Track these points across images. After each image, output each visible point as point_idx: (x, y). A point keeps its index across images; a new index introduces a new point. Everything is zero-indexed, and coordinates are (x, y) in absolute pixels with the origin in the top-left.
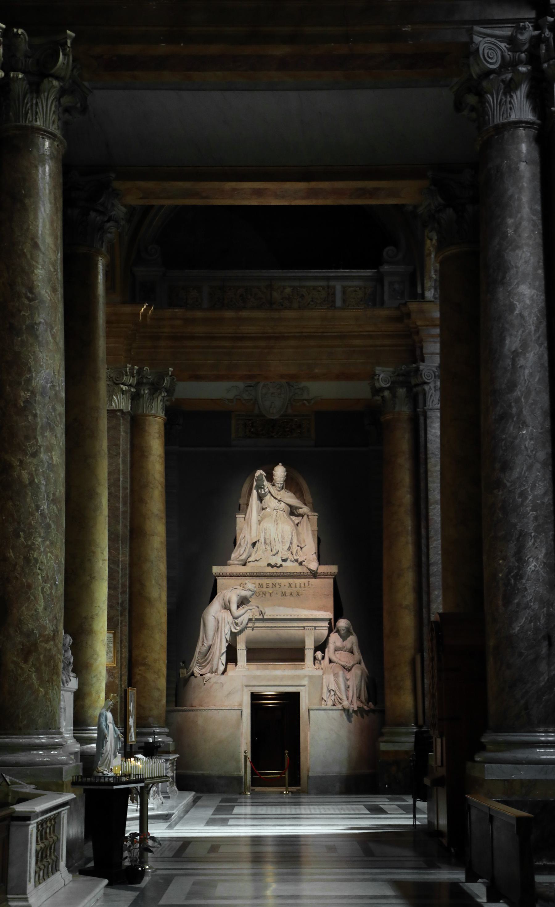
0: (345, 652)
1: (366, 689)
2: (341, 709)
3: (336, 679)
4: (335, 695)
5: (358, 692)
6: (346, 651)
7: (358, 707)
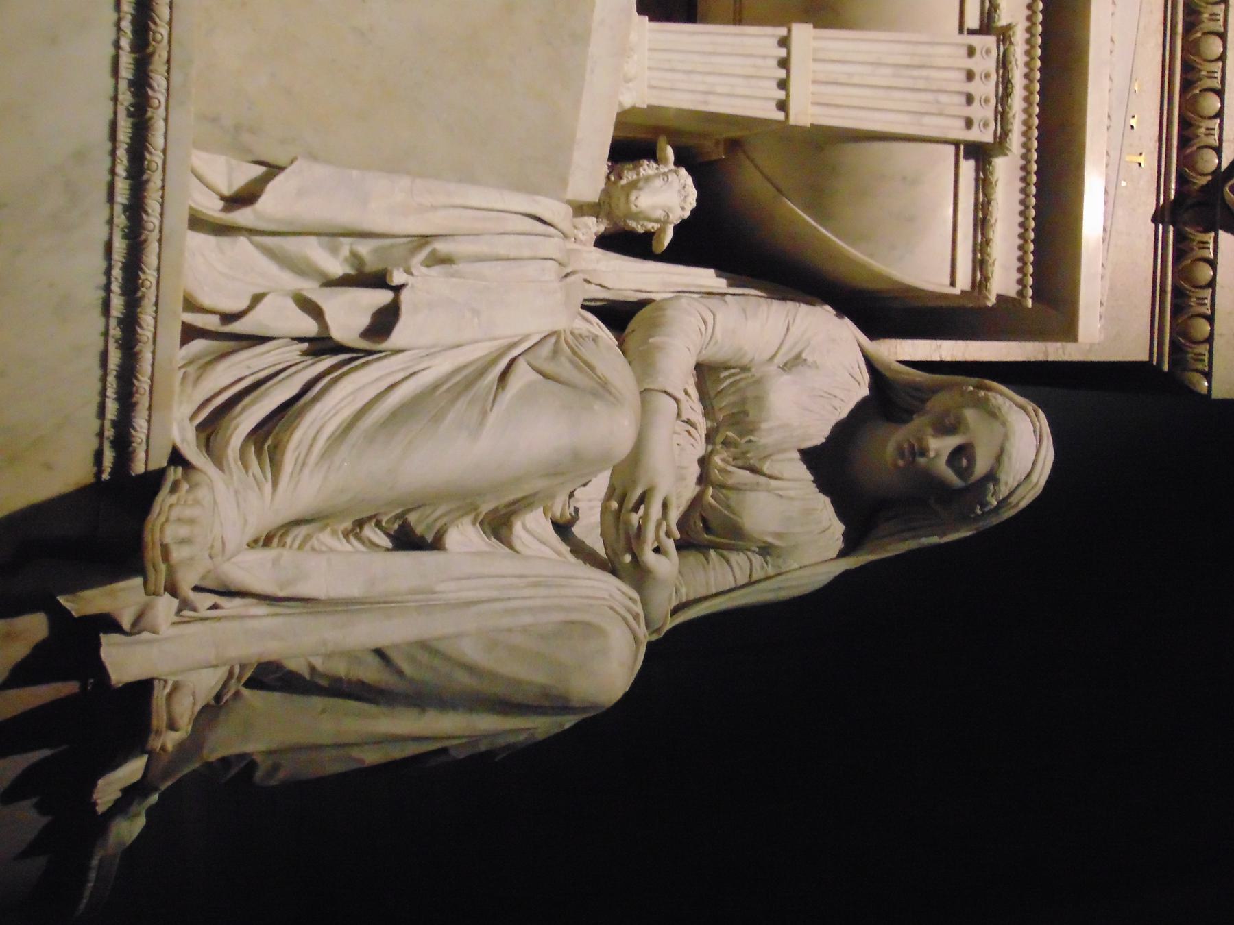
0: (695, 470)
1: (372, 757)
2: (123, 443)
3: (523, 376)
4: (321, 345)
5: (340, 668)
6: (703, 480)
7: (143, 689)
